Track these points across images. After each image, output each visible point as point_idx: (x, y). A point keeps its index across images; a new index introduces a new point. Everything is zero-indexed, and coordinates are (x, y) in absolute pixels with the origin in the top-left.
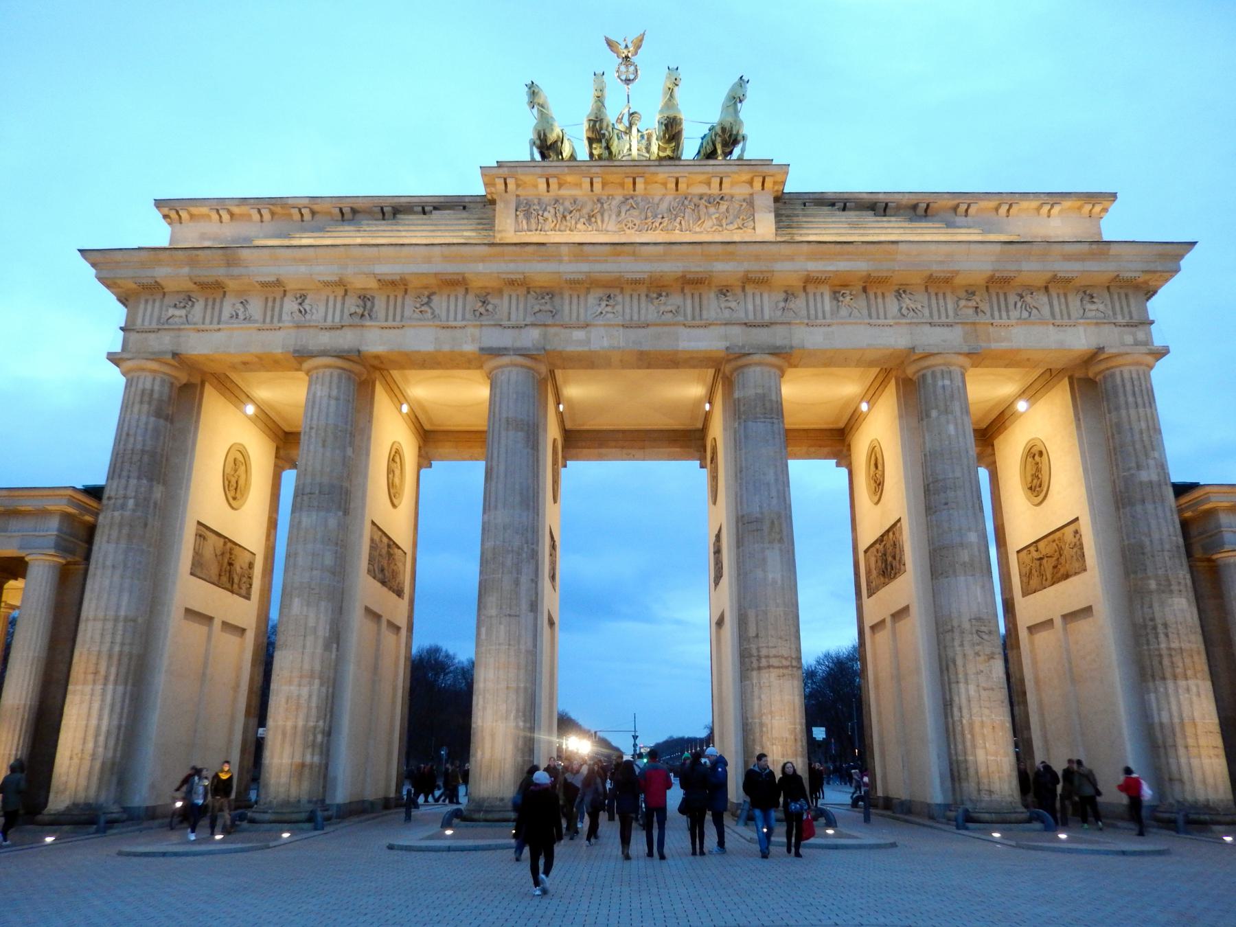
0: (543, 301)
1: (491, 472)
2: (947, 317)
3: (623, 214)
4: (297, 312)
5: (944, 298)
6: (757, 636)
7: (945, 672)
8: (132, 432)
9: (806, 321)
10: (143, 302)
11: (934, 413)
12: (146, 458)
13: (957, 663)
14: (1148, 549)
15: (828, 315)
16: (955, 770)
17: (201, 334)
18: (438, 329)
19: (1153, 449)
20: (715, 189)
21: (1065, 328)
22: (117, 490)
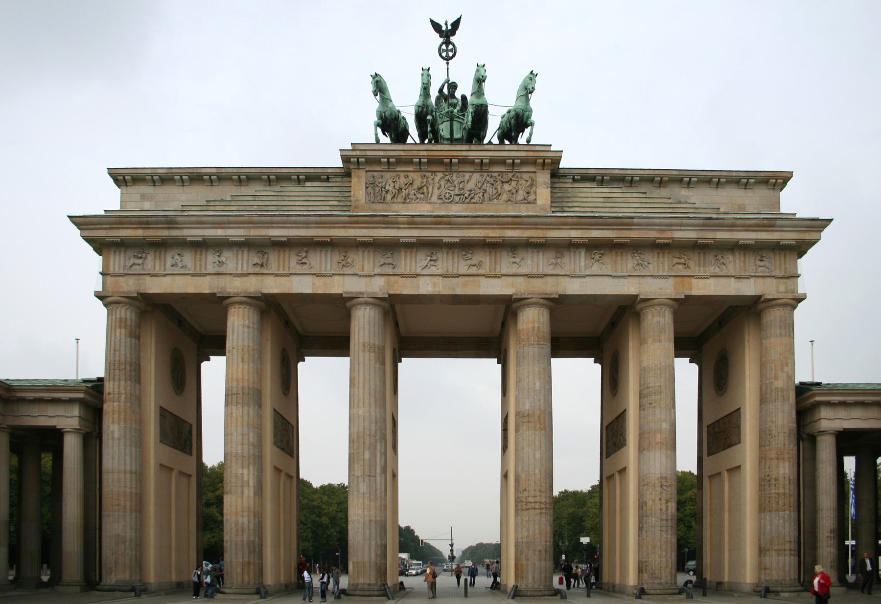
0: (386, 256)
1: (354, 380)
2: (663, 272)
3: (443, 186)
4: (218, 263)
5: (663, 258)
6: (525, 490)
7: (641, 509)
8: (117, 348)
9: (568, 274)
10: (112, 252)
11: (650, 341)
12: (128, 367)
13: (648, 504)
14: (774, 432)
15: (583, 269)
16: (640, 566)
17: (155, 278)
18: (314, 276)
19: (786, 366)
20: (510, 169)
21: (742, 280)
22: (114, 389)
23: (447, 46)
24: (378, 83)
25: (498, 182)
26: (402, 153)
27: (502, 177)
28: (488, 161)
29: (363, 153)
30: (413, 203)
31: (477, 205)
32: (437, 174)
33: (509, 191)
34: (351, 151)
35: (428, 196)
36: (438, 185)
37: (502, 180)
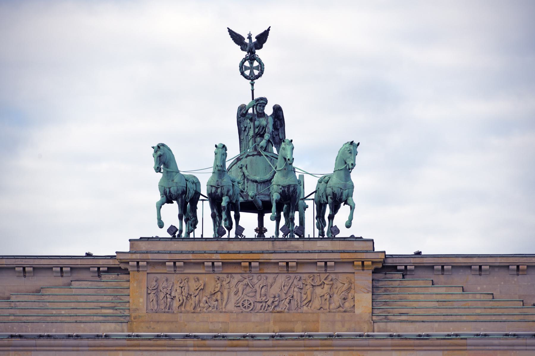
3: (240, 292)
23: (251, 63)
24: (162, 157)
25: (308, 287)
26: (191, 256)
27: (313, 280)
28: (294, 264)
29: (144, 256)
30: (205, 313)
31: (282, 314)
32: (234, 275)
33: (321, 297)
34: (130, 255)
35: (222, 303)
36: (235, 290)
37: (313, 284)
